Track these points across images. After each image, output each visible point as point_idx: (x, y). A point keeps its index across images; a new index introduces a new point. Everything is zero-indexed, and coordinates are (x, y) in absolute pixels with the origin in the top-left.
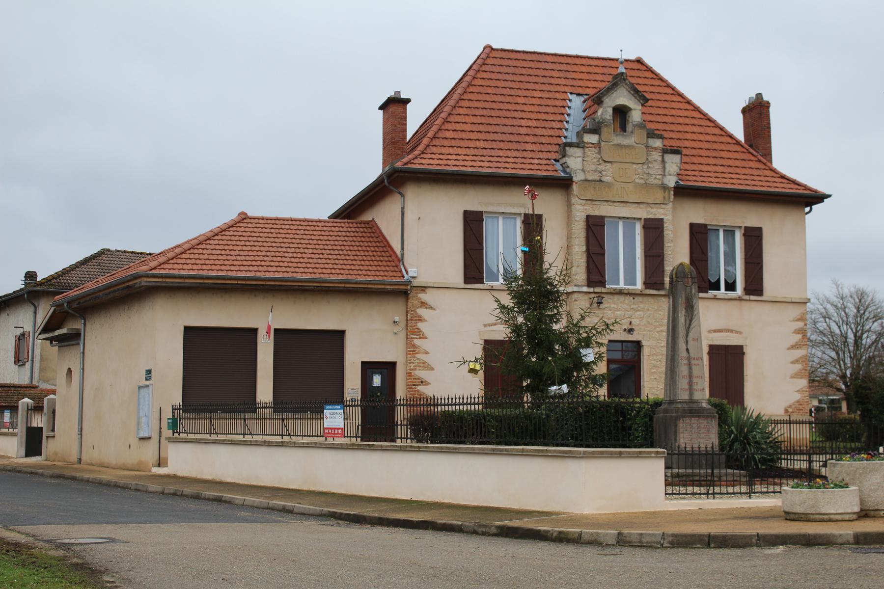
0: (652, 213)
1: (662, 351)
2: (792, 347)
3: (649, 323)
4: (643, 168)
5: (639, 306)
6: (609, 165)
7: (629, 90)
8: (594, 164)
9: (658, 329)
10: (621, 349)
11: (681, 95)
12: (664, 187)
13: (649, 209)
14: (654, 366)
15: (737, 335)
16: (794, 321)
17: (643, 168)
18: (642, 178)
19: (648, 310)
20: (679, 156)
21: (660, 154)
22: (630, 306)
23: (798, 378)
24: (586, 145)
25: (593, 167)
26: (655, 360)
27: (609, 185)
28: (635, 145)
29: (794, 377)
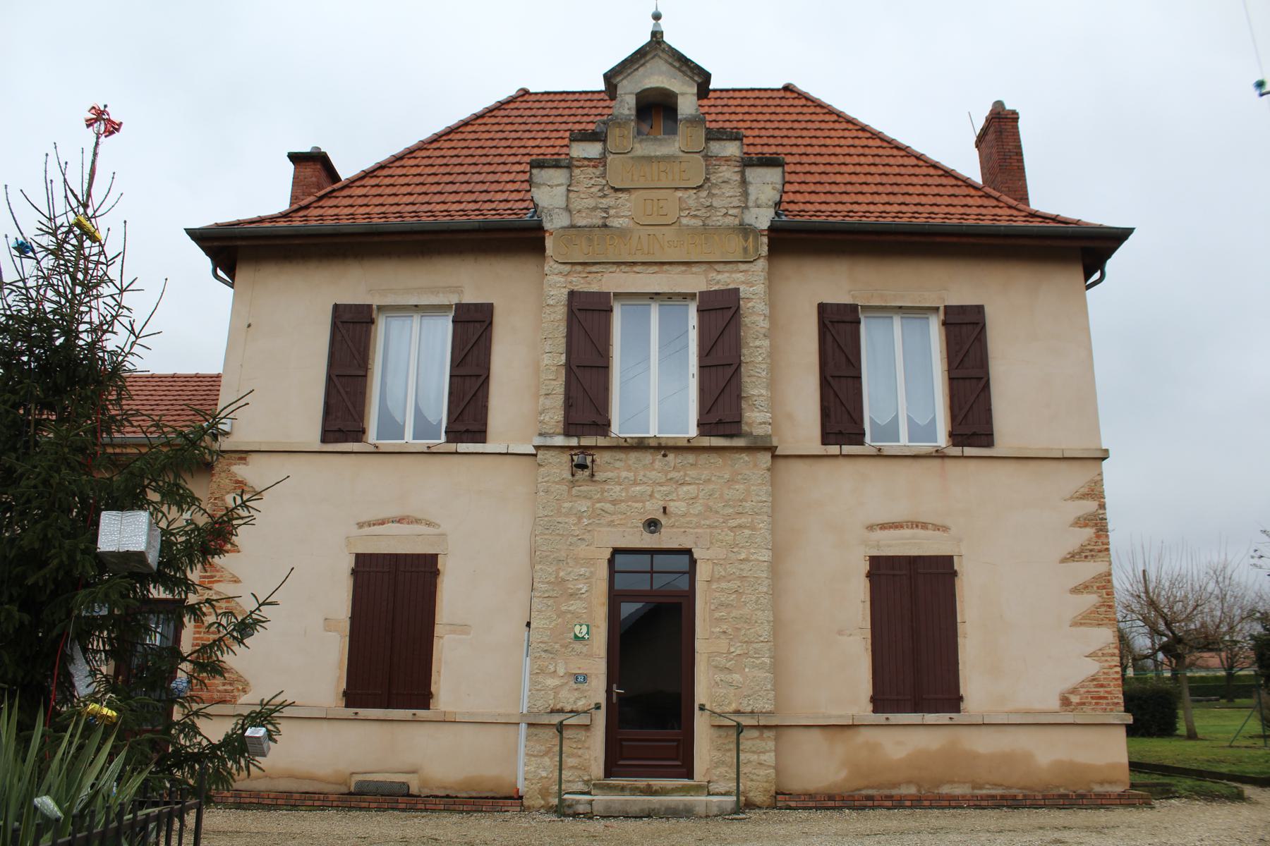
0: (718, 282)
1: (742, 570)
2: (1073, 557)
3: (709, 508)
4: (698, 198)
5: (686, 475)
6: (624, 196)
7: (670, 60)
8: (592, 195)
9: (732, 523)
11: (851, 121)
12: (745, 230)
13: (714, 274)
15: (937, 532)
16: (1072, 498)
17: (698, 198)
18: (695, 216)
19: (708, 481)
20: (779, 170)
21: (737, 169)
22: (666, 476)
23: (1091, 625)
24: (576, 163)
25: (591, 202)
26: (722, 590)
27: (623, 233)
28: (681, 154)
29: (1081, 624)
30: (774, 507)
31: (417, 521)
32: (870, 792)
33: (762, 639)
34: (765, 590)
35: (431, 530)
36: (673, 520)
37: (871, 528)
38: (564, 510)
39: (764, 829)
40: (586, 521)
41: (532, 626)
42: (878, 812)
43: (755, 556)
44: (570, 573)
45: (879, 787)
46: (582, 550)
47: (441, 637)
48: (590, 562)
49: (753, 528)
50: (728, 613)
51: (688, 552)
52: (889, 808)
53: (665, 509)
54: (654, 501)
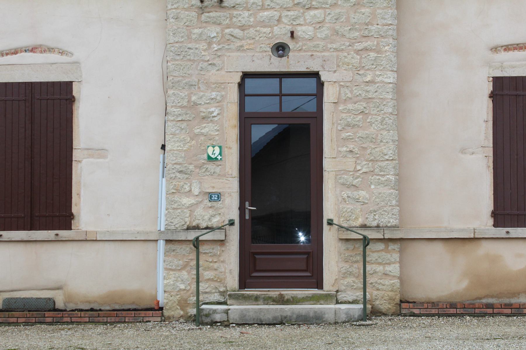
1: (368, 92)
9: (358, 46)
10: (278, 92)
14: (348, 125)
26: (349, 111)
30: (398, 31)
31: (50, 50)
32: (491, 301)
33: (387, 157)
34: (390, 110)
35: (64, 59)
36: (300, 44)
37: (495, 49)
38: (194, 37)
39: (389, 333)
40: (215, 47)
41: (167, 148)
42: (498, 319)
43: (380, 78)
44: (201, 98)
45: (498, 296)
46: (213, 75)
47: (80, 162)
48: (220, 86)
49: (379, 52)
50: (354, 133)
51: (316, 75)
52: (508, 316)
53: (292, 33)
54: (282, 26)
